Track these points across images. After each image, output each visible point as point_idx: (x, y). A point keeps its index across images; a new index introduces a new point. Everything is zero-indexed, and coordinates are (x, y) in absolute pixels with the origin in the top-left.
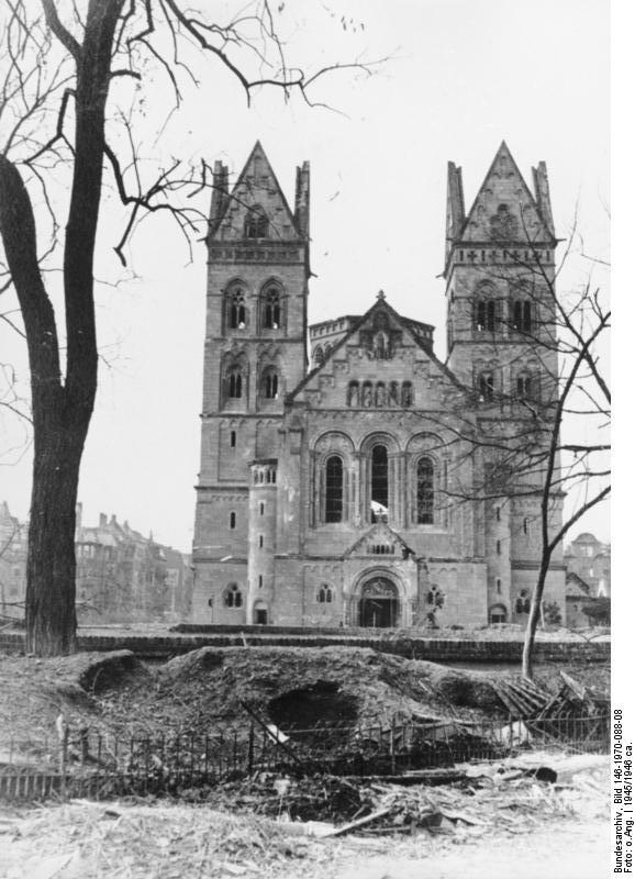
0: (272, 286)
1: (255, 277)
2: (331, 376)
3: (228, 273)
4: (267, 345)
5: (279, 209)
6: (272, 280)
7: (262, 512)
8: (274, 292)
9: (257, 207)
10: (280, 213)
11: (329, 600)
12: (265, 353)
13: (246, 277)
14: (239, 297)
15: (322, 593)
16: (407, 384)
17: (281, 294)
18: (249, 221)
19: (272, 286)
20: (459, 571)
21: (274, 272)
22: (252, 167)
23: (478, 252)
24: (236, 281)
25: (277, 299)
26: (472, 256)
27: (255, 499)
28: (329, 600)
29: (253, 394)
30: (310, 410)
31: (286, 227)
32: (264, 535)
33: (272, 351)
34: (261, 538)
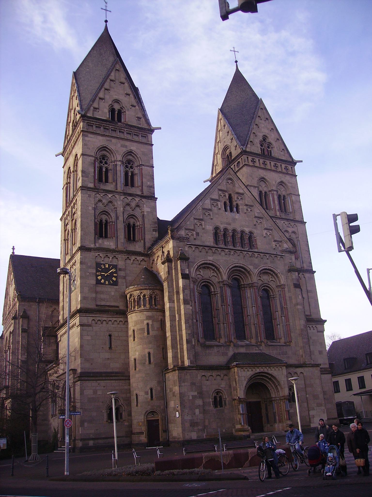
0: (130, 157)
1: (118, 148)
2: (202, 220)
3: (98, 141)
4: (130, 198)
5: (133, 106)
6: (130, 153)
7: (148, 333)
8: (129, 162)
9: (117, 101)
10: (133, 108)
11: (221, 406)
12: (128, 204)
13: (112, 147)
14: (104, 161)
15: (215, 398)
16: (251, 233)
17: (136, 164)
18: (112, 111)
19: (130, 157)
20: (305, 374)
21: (134, 147)
22: (113, 74)
23: (257, 160)
24: (104, 148)
25: (132, 167)
26: (253, 161)
27: (135, 319)
28: (221, 406)
29: (121, 235)
30: (190, 246)
31: (139, 118)
32: (152, 351)
33: (133, 204)
34: (149, 354)
